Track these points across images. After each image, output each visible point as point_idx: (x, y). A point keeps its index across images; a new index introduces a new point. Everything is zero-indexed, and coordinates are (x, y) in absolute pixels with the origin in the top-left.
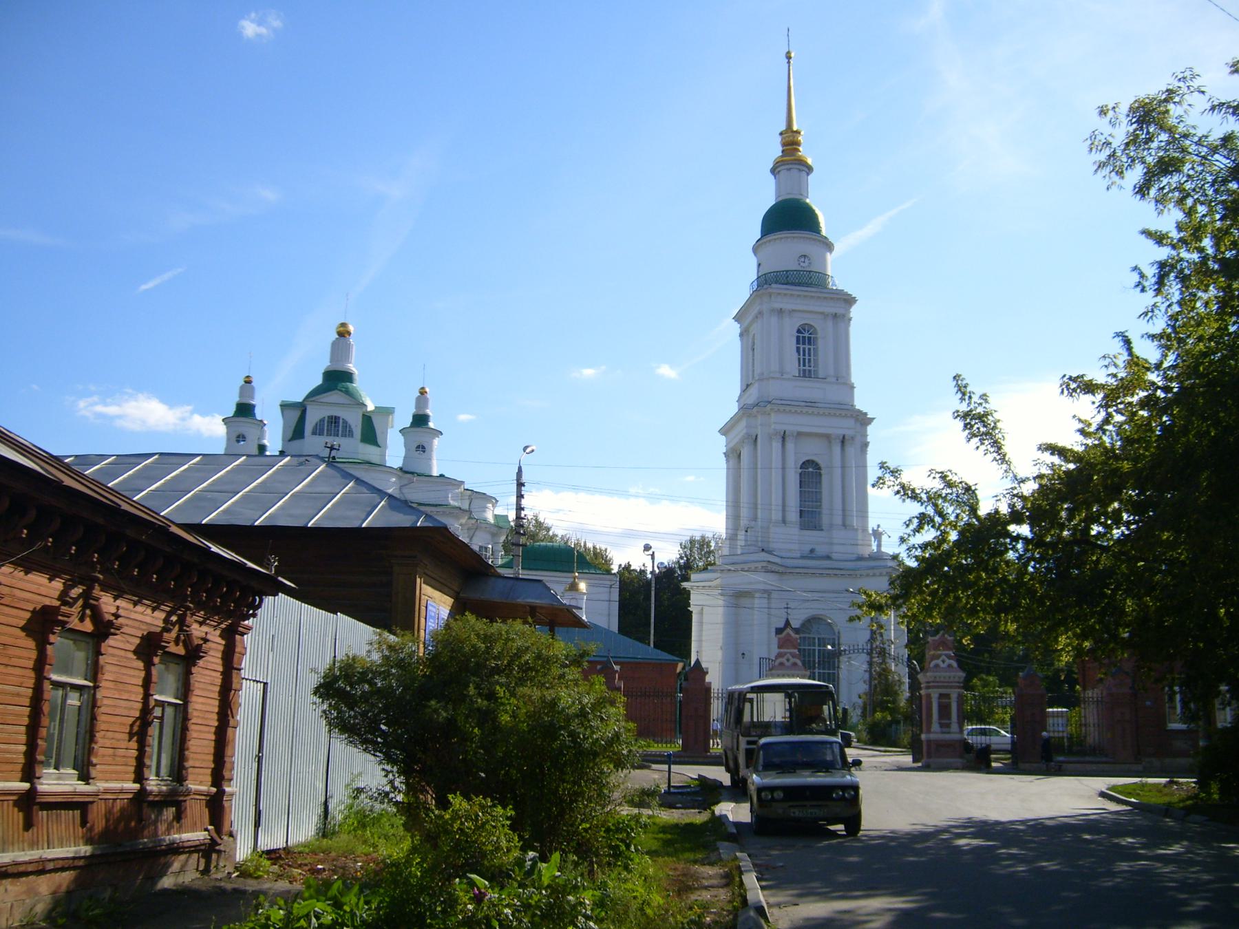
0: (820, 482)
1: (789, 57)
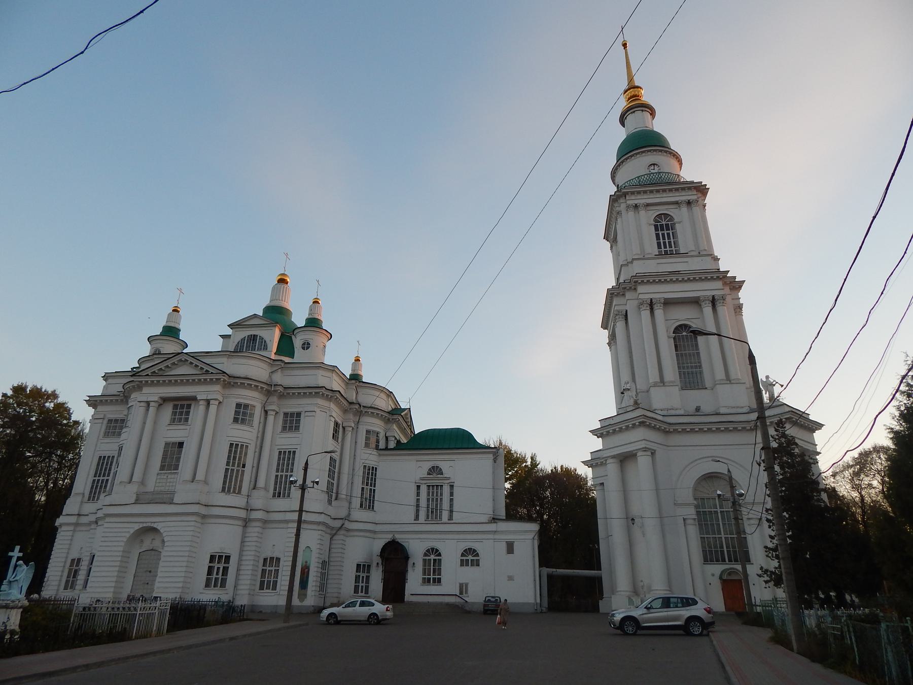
0: (697, 345)
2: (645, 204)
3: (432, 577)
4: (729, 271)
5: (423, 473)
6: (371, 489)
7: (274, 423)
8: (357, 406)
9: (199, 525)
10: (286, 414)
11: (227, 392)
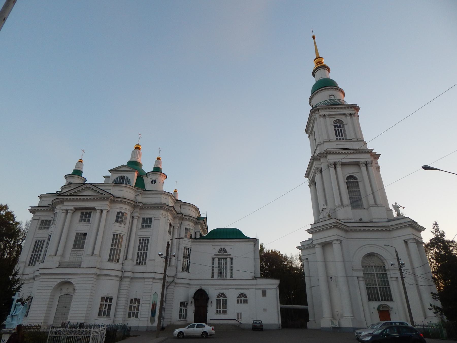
0: (358, 186)
1: (314, 37)
2: (329, 114)
3: (221, 309)
4: (374, 149)
5: (216, 252)
6: (188, 261)
7: (137, 223)
8: (181, 215)
9: (95, 280)
10: (144, 219)
11: (112, 205)
